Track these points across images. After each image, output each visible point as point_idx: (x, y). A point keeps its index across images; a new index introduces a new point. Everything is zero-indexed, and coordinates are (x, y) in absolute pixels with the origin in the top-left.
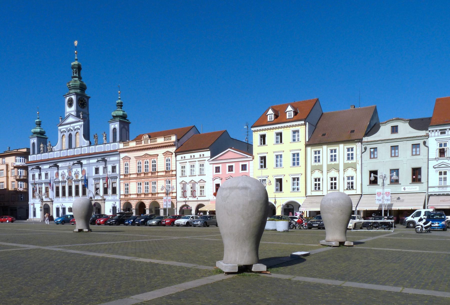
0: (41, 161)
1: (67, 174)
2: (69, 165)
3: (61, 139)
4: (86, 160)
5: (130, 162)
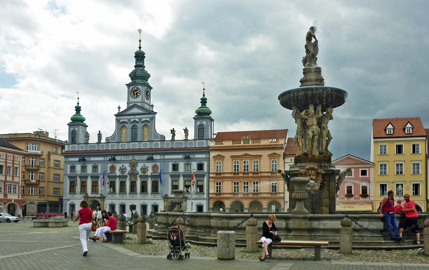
0: (86, 151)
1: (129, 169)
2: (132, 159)
3: (120, 130)
4: (159, 155)
5: (224, 161)
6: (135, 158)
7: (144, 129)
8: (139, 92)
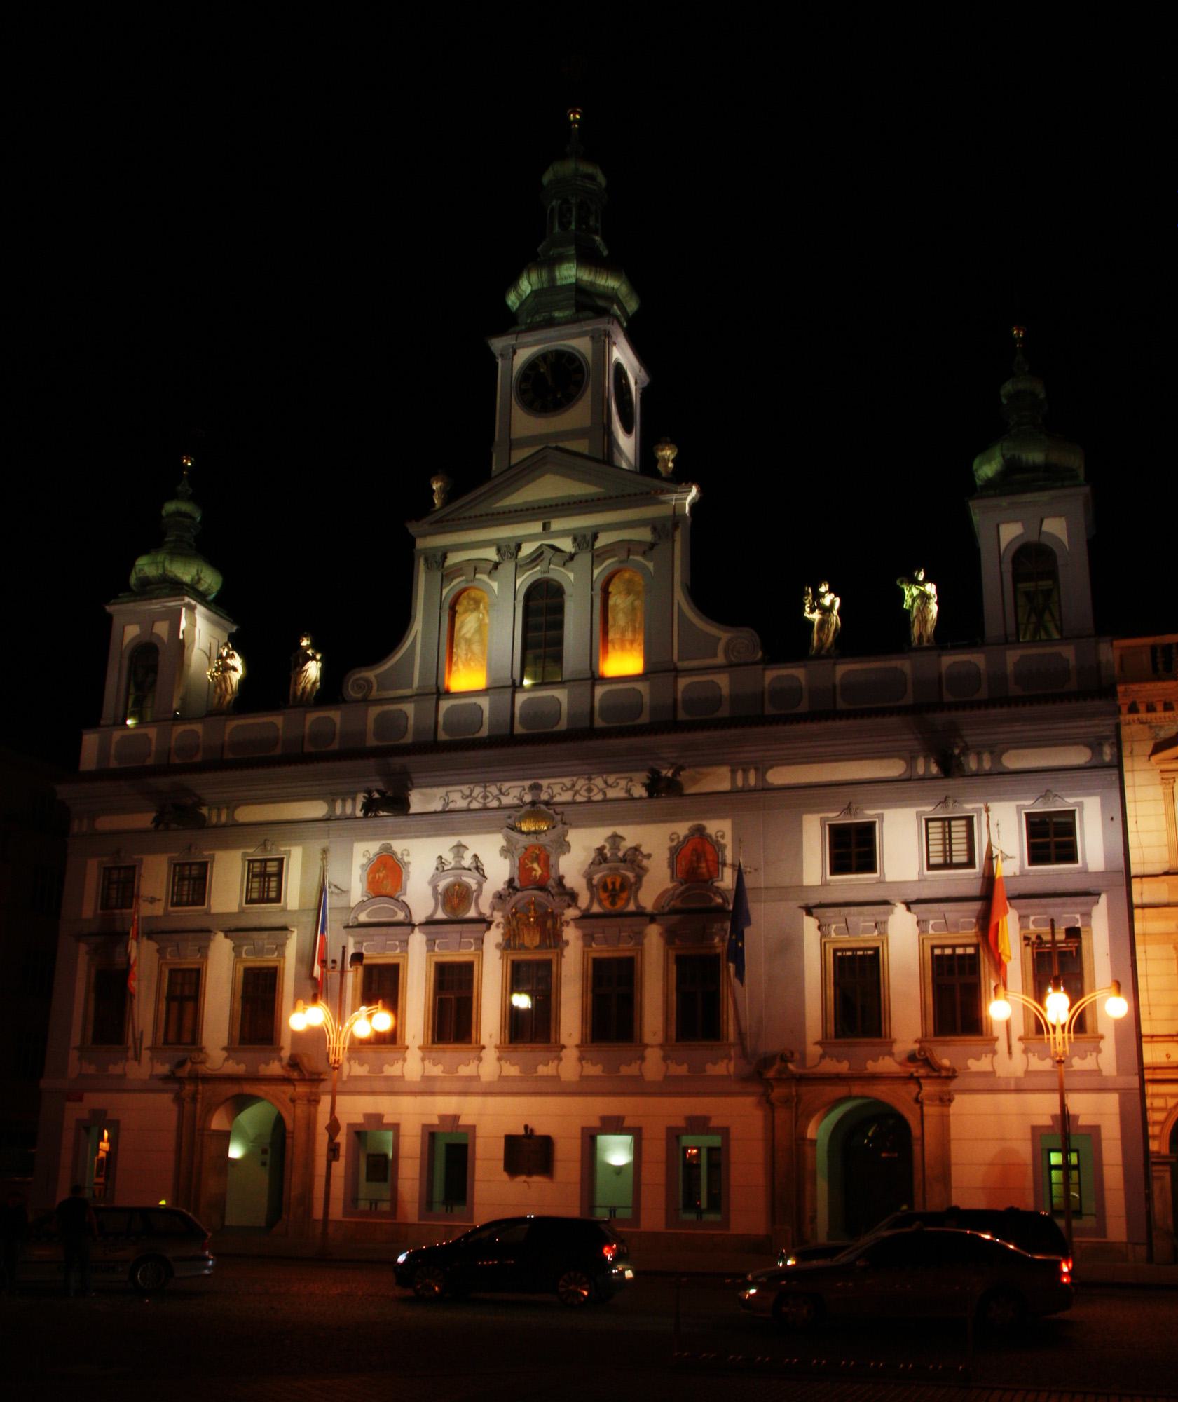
1: (499, 870)
2: (528, 798)
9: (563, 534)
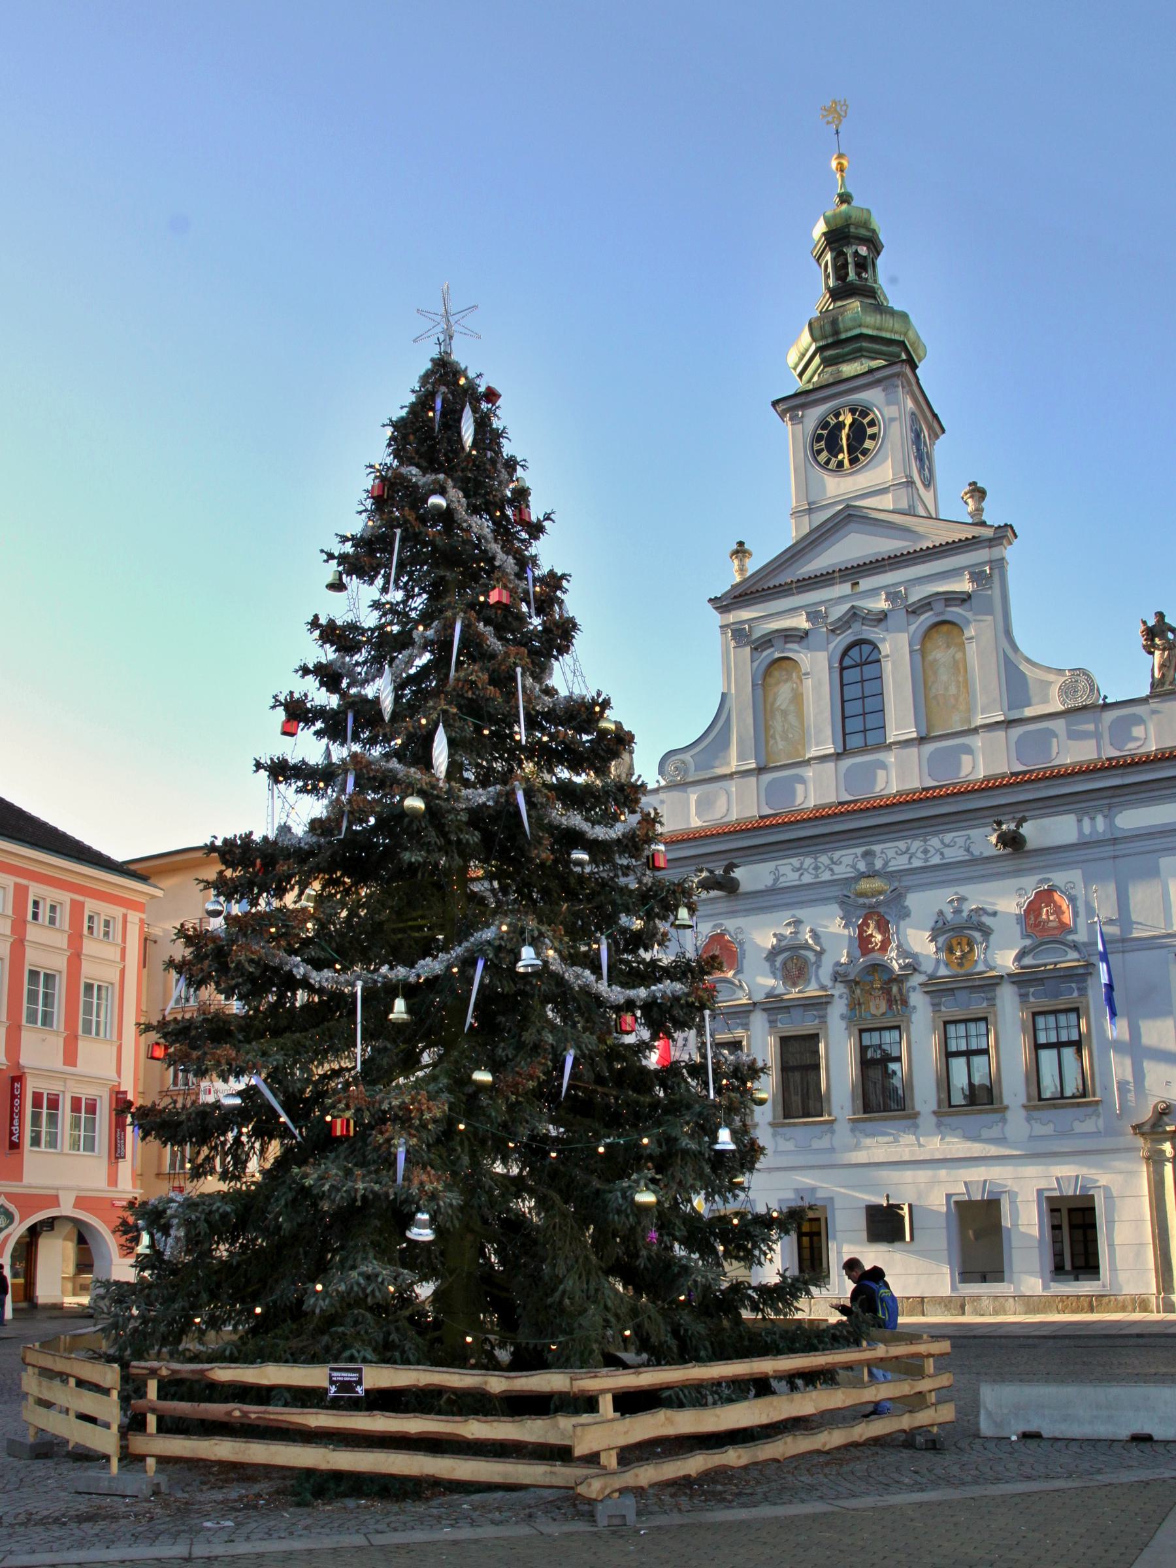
2: (862, 866)
6: (878, 864)
7: (930, 658)
8: (870, 431)
9: (874, 592)
